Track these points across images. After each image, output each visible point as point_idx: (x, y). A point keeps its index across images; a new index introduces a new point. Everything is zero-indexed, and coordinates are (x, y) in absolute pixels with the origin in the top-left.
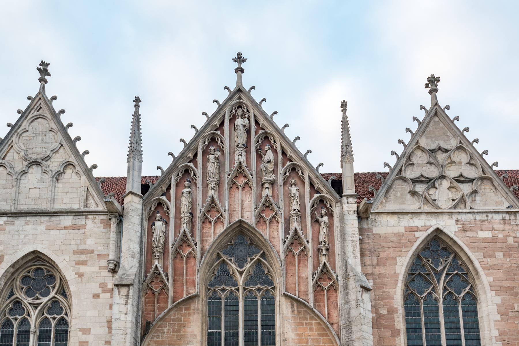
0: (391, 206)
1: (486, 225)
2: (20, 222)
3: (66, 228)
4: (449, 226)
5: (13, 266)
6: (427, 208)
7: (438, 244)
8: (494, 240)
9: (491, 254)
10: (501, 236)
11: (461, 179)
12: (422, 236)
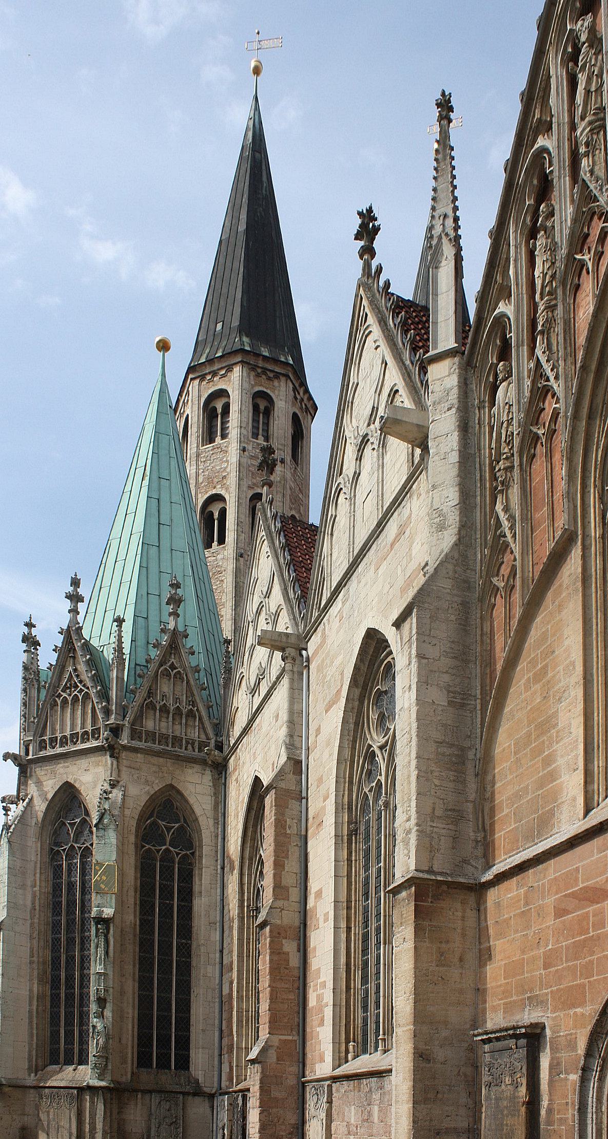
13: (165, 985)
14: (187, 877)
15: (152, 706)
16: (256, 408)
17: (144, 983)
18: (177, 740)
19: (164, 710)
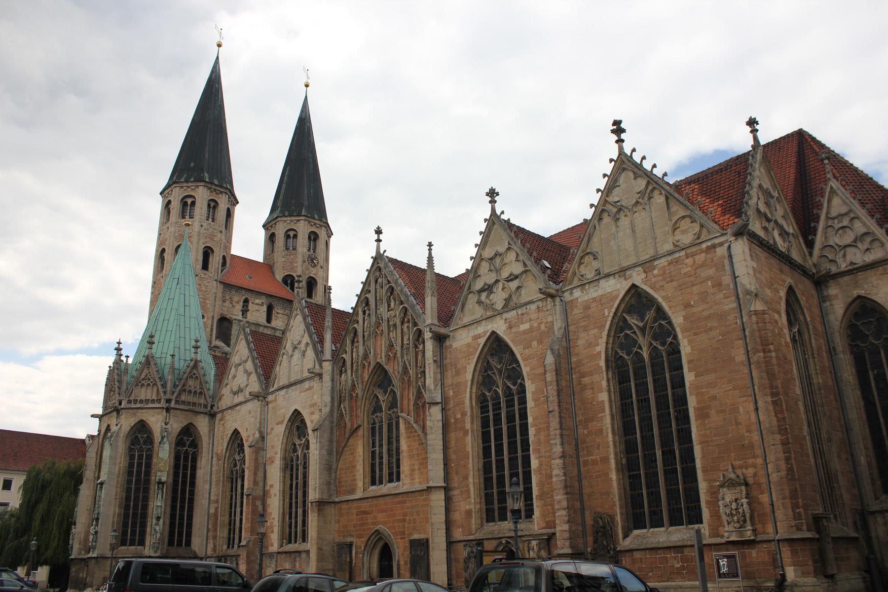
0: (466, 320)
1: (526, 317)
2: (290, 390)
3: (307, 390)
4: (499, 326)
5: (289, 420)
6: (489, 313)
7: (496, 346)
8: (531, 330)
9: (528, 346)
10: (536, 325)
11: (512, 278)
12: (482, 341)
13: (182, 508)
14: (195, 460)
15: (185, 390)
16: (209, 205)
17: (173, 508)
18: (194, 404)
19: (190, 392)
